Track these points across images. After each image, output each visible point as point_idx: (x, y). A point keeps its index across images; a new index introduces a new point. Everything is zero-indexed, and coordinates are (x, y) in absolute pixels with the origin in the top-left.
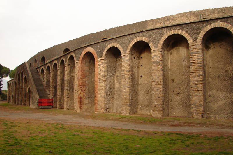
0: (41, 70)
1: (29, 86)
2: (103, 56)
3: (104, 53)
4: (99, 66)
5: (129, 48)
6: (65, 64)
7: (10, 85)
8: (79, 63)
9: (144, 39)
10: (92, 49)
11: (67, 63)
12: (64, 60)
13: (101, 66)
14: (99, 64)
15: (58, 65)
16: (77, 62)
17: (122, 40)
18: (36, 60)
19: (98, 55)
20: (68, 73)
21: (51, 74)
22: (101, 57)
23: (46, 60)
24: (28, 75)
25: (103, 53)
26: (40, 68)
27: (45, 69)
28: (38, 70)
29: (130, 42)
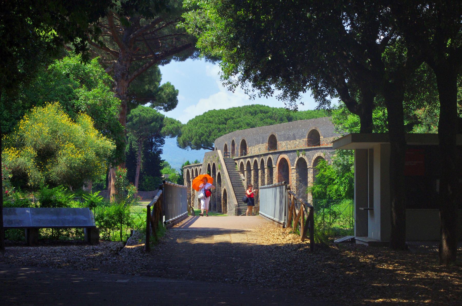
0: (240, 164)
1: (225, 187)
2: (295, 165)
3: (296, 162)
4: (292, 175)
5: (313, 161)
6: (265, 165)
7: (191, 174)
8: (276, 168)
9: (322, 155)
10: (287, 155)
11: (266, 165)
12: (264, 160)
13: (294, 175)
14: (292, 172)
15: (259, 163)
16: (275, 166)
17: (308, 153)
18: (233, 141)
19: (291, 164)
20: (268, 176)
21: (252, 172)
22: (293, 166)
23: (247, 145)
24: (222, 171)
25: (294, 162)
26: (239, 161)
27: (245, 164)
28: (236, 162)
29: (313, 156)
